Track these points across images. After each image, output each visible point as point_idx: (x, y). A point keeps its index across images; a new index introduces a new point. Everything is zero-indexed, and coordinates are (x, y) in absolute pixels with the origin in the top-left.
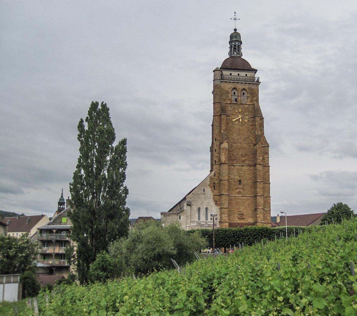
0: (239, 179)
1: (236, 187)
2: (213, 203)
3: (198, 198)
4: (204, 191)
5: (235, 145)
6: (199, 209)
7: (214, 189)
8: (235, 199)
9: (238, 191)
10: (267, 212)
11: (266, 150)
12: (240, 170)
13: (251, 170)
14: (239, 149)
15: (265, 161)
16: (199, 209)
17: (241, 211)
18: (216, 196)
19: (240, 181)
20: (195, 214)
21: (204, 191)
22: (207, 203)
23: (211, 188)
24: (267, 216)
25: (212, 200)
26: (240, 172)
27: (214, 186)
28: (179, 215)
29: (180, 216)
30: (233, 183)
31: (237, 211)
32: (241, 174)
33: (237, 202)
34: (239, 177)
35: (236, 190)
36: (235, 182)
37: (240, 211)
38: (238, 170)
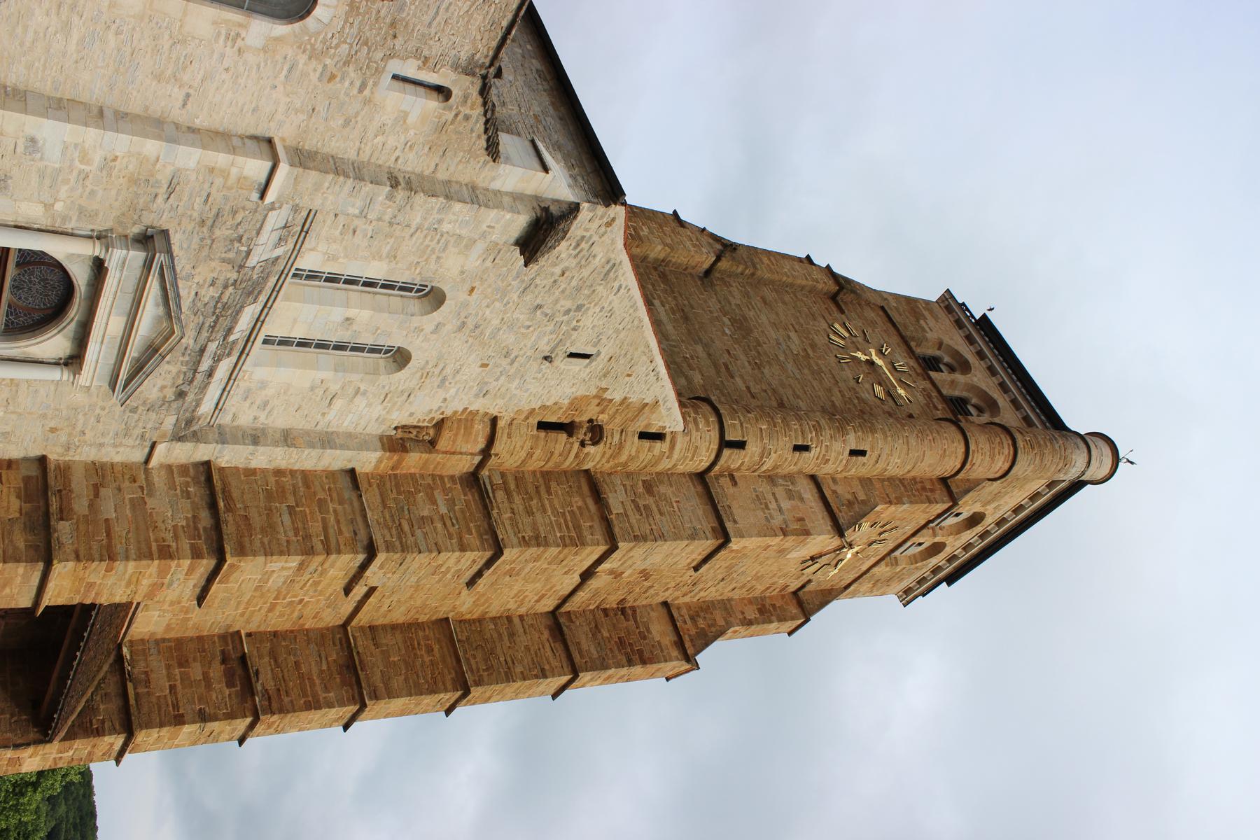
2: (421, 408)
3: (539, 307)
4: (572, 355)
6: (433, 297)
7: (543, 426)
13: (538, 601)
16: (433, 297)
18: (481, 444)
20: (393, 257)
21: (572, 355)
22: (448, 371)
23: (566, 402)
25: (455, 406)
27: (568, 428)
28: (464, 87)
29: (443, 92)
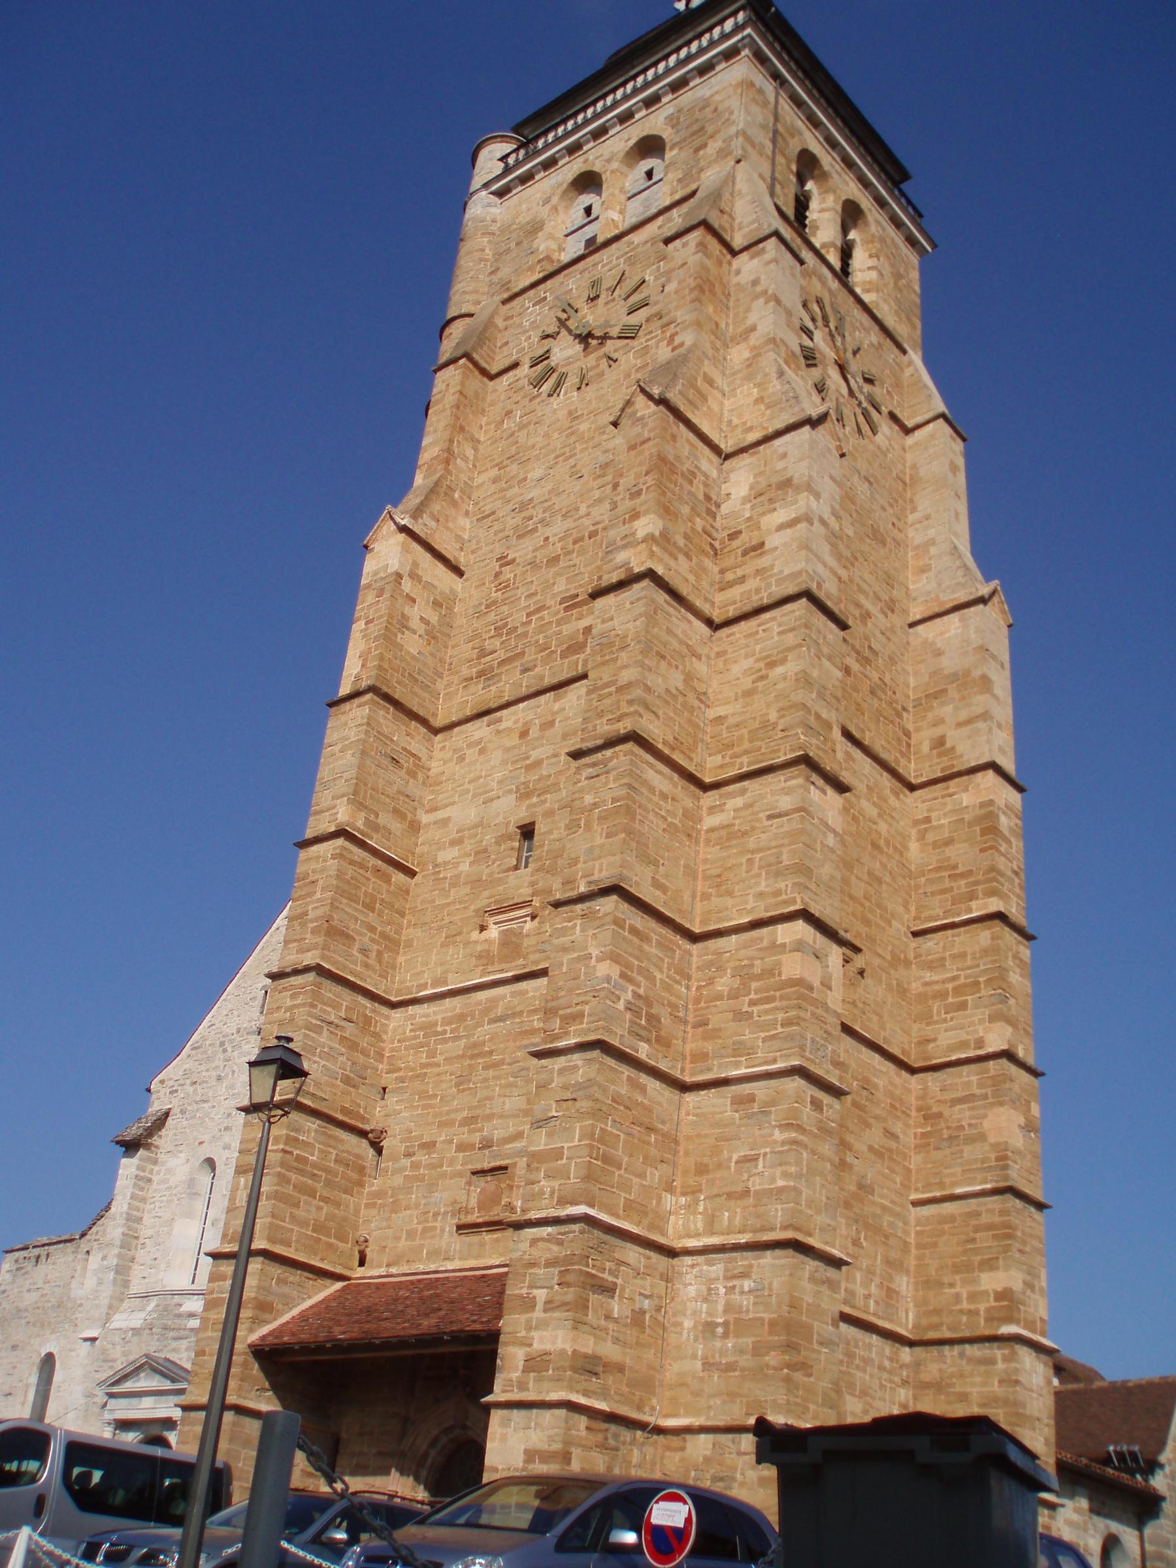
0: (522, 815)
1: (484, 900)
5: (522, 551)
8: (462, 1017)
9: (493, 932)
10: (751, 1099)
11: (780, 465)
12: (534, 732)
14: (555, 560)
15: (764, 561)
17: (497, 1134)
19: (527, 832)
24: (753, 1159)
26: (535, 755)
30: (465, 867)
31: (461, 1148)
32: (538, 763)
33: (475, 1051)
34: (524, 794)
35: (475, 935)
36: (481, 854)
37: (487, 1144)
38: (524, 734)
